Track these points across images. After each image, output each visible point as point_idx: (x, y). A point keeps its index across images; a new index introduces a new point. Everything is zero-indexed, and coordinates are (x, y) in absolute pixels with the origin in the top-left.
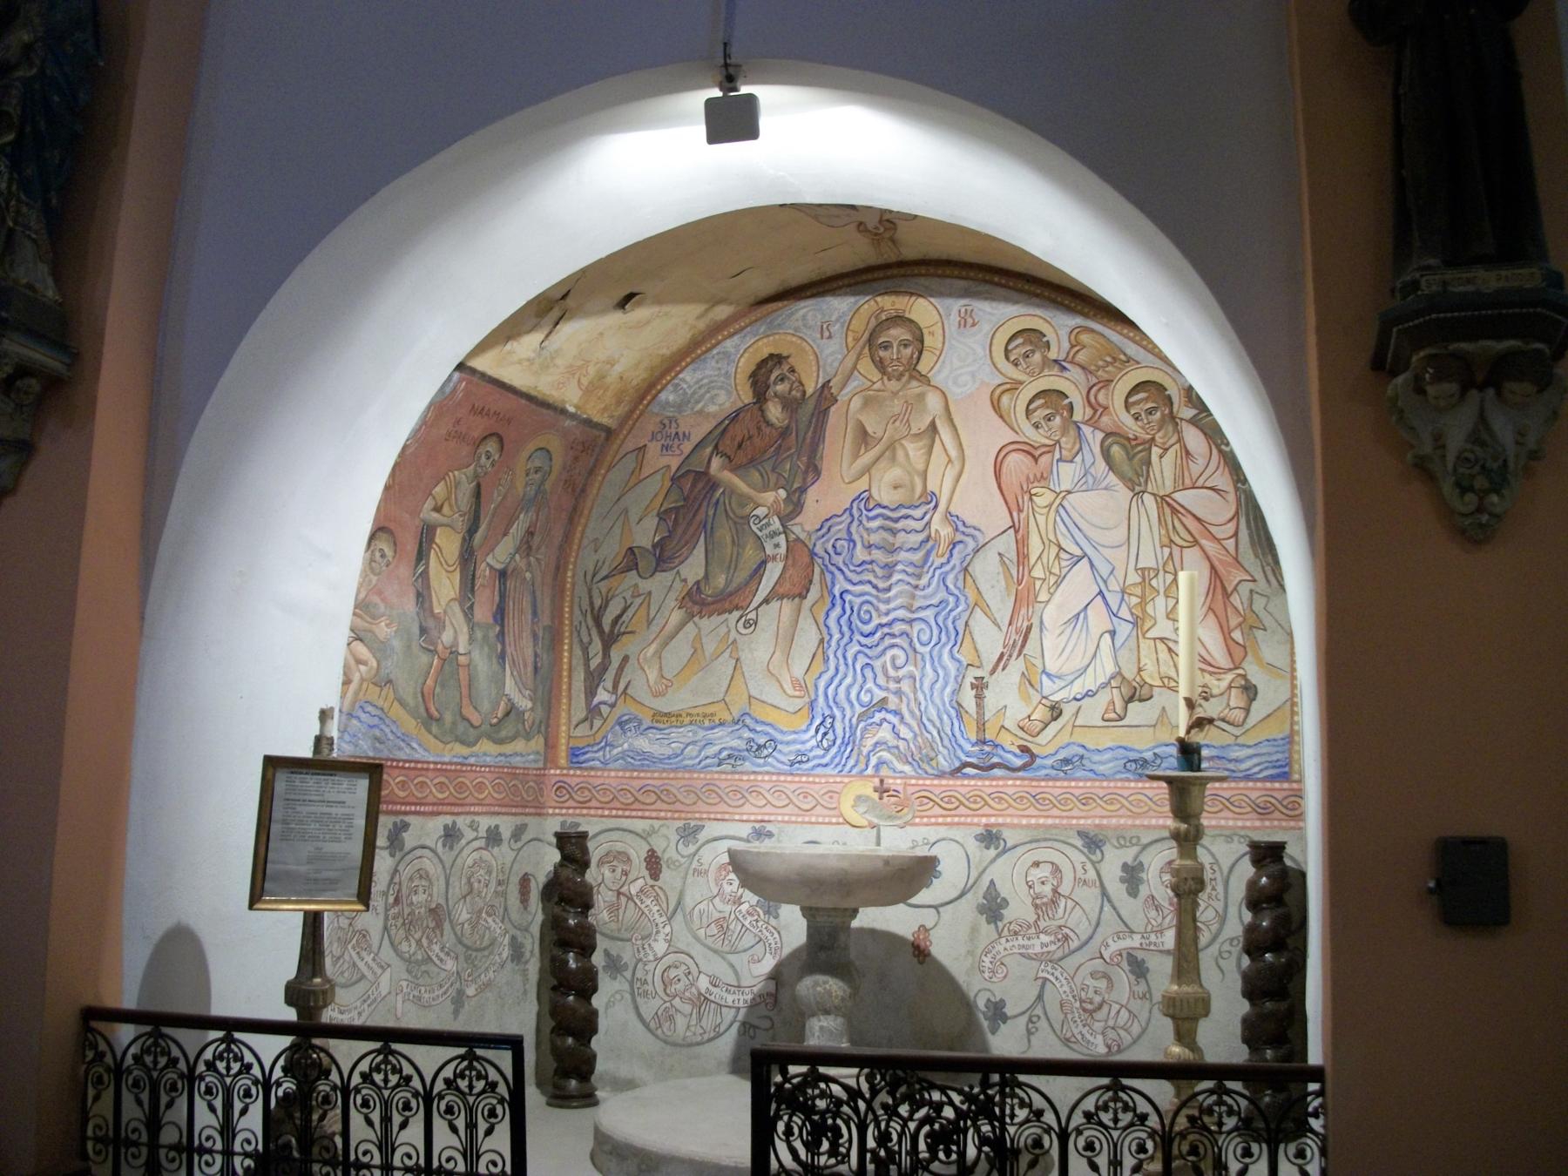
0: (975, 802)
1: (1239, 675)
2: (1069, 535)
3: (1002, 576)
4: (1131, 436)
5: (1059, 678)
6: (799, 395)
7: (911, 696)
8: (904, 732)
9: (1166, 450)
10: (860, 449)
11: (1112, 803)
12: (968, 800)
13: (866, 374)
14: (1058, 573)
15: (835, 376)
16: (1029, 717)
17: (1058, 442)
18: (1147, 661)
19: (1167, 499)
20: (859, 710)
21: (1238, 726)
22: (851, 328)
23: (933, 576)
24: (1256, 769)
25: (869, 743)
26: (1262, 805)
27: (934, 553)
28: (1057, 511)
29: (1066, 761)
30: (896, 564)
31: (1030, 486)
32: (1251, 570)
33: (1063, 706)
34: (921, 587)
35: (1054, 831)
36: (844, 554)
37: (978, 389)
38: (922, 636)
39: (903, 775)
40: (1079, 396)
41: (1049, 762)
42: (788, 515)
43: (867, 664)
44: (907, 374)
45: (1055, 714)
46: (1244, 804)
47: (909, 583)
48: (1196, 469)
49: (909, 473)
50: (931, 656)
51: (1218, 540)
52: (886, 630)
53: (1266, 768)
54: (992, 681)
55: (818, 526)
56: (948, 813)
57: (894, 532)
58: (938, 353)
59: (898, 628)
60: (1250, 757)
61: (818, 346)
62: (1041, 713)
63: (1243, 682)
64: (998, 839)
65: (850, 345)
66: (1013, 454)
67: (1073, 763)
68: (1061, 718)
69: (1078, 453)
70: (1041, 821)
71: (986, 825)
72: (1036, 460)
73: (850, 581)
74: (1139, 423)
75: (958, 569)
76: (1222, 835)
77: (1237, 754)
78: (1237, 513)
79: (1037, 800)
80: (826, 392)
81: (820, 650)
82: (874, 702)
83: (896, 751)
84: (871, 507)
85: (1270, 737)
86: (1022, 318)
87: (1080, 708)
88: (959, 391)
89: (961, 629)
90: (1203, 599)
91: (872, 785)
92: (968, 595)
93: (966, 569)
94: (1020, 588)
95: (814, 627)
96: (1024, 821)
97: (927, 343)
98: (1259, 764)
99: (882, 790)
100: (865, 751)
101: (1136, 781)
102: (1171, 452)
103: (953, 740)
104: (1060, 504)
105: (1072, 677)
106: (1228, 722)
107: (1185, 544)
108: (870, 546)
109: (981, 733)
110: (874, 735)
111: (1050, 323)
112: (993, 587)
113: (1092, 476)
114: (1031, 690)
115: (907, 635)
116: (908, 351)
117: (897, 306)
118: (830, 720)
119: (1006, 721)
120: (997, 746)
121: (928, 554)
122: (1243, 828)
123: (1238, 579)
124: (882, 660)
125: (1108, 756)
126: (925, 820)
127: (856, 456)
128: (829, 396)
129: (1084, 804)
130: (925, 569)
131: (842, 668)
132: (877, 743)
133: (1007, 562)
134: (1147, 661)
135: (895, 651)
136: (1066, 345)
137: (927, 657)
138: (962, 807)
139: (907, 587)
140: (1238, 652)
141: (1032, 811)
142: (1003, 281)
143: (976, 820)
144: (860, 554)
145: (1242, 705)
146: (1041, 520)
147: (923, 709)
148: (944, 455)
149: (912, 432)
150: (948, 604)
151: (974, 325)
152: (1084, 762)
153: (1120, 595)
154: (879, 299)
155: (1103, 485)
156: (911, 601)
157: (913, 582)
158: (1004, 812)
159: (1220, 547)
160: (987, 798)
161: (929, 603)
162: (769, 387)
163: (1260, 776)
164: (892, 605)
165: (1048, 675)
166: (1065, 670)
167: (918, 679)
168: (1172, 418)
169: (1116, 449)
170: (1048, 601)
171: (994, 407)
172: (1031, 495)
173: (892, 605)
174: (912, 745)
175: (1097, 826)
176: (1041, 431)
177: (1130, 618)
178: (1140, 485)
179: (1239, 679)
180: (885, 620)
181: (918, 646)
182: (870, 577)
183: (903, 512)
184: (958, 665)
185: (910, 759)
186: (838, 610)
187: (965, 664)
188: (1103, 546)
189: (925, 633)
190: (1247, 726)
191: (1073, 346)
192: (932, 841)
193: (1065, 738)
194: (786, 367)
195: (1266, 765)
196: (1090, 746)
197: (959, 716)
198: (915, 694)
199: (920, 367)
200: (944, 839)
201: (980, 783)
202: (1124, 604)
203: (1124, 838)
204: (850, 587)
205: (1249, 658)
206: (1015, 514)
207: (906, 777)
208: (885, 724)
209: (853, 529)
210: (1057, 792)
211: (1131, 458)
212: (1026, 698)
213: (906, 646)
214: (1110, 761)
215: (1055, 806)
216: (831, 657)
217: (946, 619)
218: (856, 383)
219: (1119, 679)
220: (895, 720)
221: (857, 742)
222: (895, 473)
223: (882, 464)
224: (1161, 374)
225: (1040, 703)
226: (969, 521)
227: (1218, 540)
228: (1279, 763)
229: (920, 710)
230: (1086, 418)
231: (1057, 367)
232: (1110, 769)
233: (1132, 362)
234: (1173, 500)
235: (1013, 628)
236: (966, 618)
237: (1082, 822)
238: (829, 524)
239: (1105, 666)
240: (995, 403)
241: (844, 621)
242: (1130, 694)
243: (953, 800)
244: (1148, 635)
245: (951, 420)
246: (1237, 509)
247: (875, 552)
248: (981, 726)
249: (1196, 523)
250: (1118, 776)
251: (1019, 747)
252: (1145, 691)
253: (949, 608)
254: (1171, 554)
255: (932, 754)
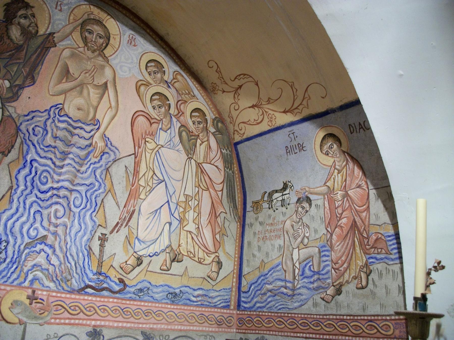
0: (90, 311)
1: (217, 256)
2: (159, 168)
3: (125, 179)
4: (191, 130)
5: (143, 242)
6: (33, 31)
7: (63, 237)
8: (54, 260)
9: (203, 142)
10: (63, 79)
11: (159, 316)
12: (86, 309)
13: (76, 41)
14: (151, 186)
15: (58, 32)
16: (126, 262)
17: (162, 120)
18: (183, 242)
19: (200, 165)
20: (27, 240)
21: (214, 281)
22: (74, 12)
23: (89, 168)
24: (219, 303)
25: (30, 264)
26: (219, 321)
27: (92, 154)
28: (156, 154)
29: (141, 290)
30: (69, 154)
31: (146, 136)
32: (226, 208)
33: (144, 259)
34: (81, 171)
35: (130, 331)
36: (39, 136)
37: (131, 77)
38: (76, 201)
39: (48, 289)
40: (173, 102)
41: (132, 290)
42: (8, 98)
43: (38, 211)
44: (98, 52)
45: (139, 263)
46: (213, 320)
47: (74, 167)
48: (212, 155)
49: (88, 104)
50: (79, 215)
51: (216, 191)
52: (55, 192)
53: (222, 302)
54: (110, 237)
55: (26, 114)
56: (73, 317)
57: (72, 134)
58: (115, 50)
59: (62, 192)
60: (217, 296)
61: (52, 11)
62: (132, 261)
63: (218, 260)
64: (99, 335)
65: (71, 21)
66: (141, 117)
67: (144, 292)
68: (141, 265)
69: (169, 129)
70: (125, 325)
71: (94, 326)
72: (151, 125)
73: (39, 154)
74: (194, 126)
75: (103, 168)
76: (202, 335)
77: (213, 294)
78: (224, 180)
79: (124, 312)
80: (51, 37)
81: (9, 193)
82: (38, 237)
83: (47, 272)
84: (62, 114)
85: (225, 288)
86: (155, 54)
87: (151, 261)
88: (121, 73)
89: (99, 203)
90: (208, 216)
91: (26, 294)
92: (107, 184)
93: (107, 169)
94: (132, 188)
95: (8, 177)
96: (116, 325)
97: (111, 42)
98: (220, 300)
99: (32, 298)
100: (25, 269)
101: (171, 304)
102: (205, 144)
103: (83, 270)
104: (158, 151)
105: (149, 244)
106: (211, 278)
107: (204, 189)
108: (56, 137)
109: (100, 268)
110: (34, 259)
111: (167, 63)
112: (119, 184)
113: (173, 142)
114: (129, 247)
115: (67, 199)
116: (101, 41)
117: (100, 16)
118: (5, 244)
119: (114, 262)
120: (107, 277)
121: (89, 154)
122: (211, 332)
123: (221, 211)
124: (49, 210)
125: (160, 289)
126: (58, 321)
127: (60, 82)
128: (52, 41)
129: (146, 316)
130: (86, 162)
131: (21, 209)
132: (35, 265)
133: (129, 172)
134: (183, 242)
135: (58, 207)
136: (171, 77)
137: (77, 215)
138: (81, 314)
139: (73, 169)
140: (217, 244)
141: (120, 319)
142: (151, 34)
143: (88, 322)
144: (49, 140)
145: (216, 271)
146: (148, 155)
147: (68, 247)
148: (108, 103)
149: (94, 83)
150: (94, 186)
151: (135, 46)
152: (150, 292)
153: (176, 205)
154: (92, 7)
155: (177, 148)
156: (74, 178)
157: (77, 167)
158: (105, 318)
159: (216, 194)
160: (97, 309)
161: (84, 182)
162: (16, 17)
163: (220, 306)
164: (62, 178)
165: (139, 240)
166: (147, 239)
167: (68, 227)
168: (206, 129)
169: (184, 134)
170: (144, 199)
171: (137, 89)
172: (146, 141)
173: (62, 178)
174: (57, 270)
175: (151, 328)
176: (155, 111)
177: (178, 219)
178: (191, 155)
179: (216, 258)
180: (55, 185)
181: (72, 207)
182: (52, 156)
183: (80, 125)
184: (93, 223)
185: (55, 279)
186: (27, 170)
187: (98, 224)
188: (172, 178)
189: (78, 200)
190: (217, 281)
191: (174, 79)
192: (60, 335)
193: (141, 277)
194: (29, 12)
195: (222, 301)
196: (153, 283)
197: (89, 255)
198: (65, 237)
199: (104, 51)
200: (67, 334)
201: (94, 299)
202: (177, 210)
203: (162, 336)
204: (38, 158)
205: (221, 248)
206: (137, 148)
207: (49, 290)
208: (43, 253)
209: (49, 123)
210: (134, 308)
211: (189, 141)
212: (127, 251)
213: (65, 205)
214: (161, 292)
215: (132, 316)
216: (16, 200)
217: (92, 195)
218: (69, 42)
219: (170, 248)
220: (49, 251)
221: (21, 263)
222: (80, 101)
223: (74, 93)
224: (205, 108)
225: (133, 255)
226: (114, 143)
227: (216, 191)
228: (227, 300)
229: (66, 248)
230: (175, 114)
231: (166, 85)
232: (160, 297)
233: (195, 98)
234: (202, 166)
235: (126, 209)
236: (103, 197)
237: (144, 326)
238: (34, 114)
239: (164, 241)
240: (138, 88)
241: (29, 179)
242: (174, 258)
243: (77, 308)
244: (185, 229)
245: (115, 86)
246: (224, 179)
247: (58, 141)
248: (100, 264)
249: (209, 180)
250: (164, 301)
251: (119, 279)
252: (180, 257)
253: (95, 189)
254: (198, 191)
255: (69, 277)
